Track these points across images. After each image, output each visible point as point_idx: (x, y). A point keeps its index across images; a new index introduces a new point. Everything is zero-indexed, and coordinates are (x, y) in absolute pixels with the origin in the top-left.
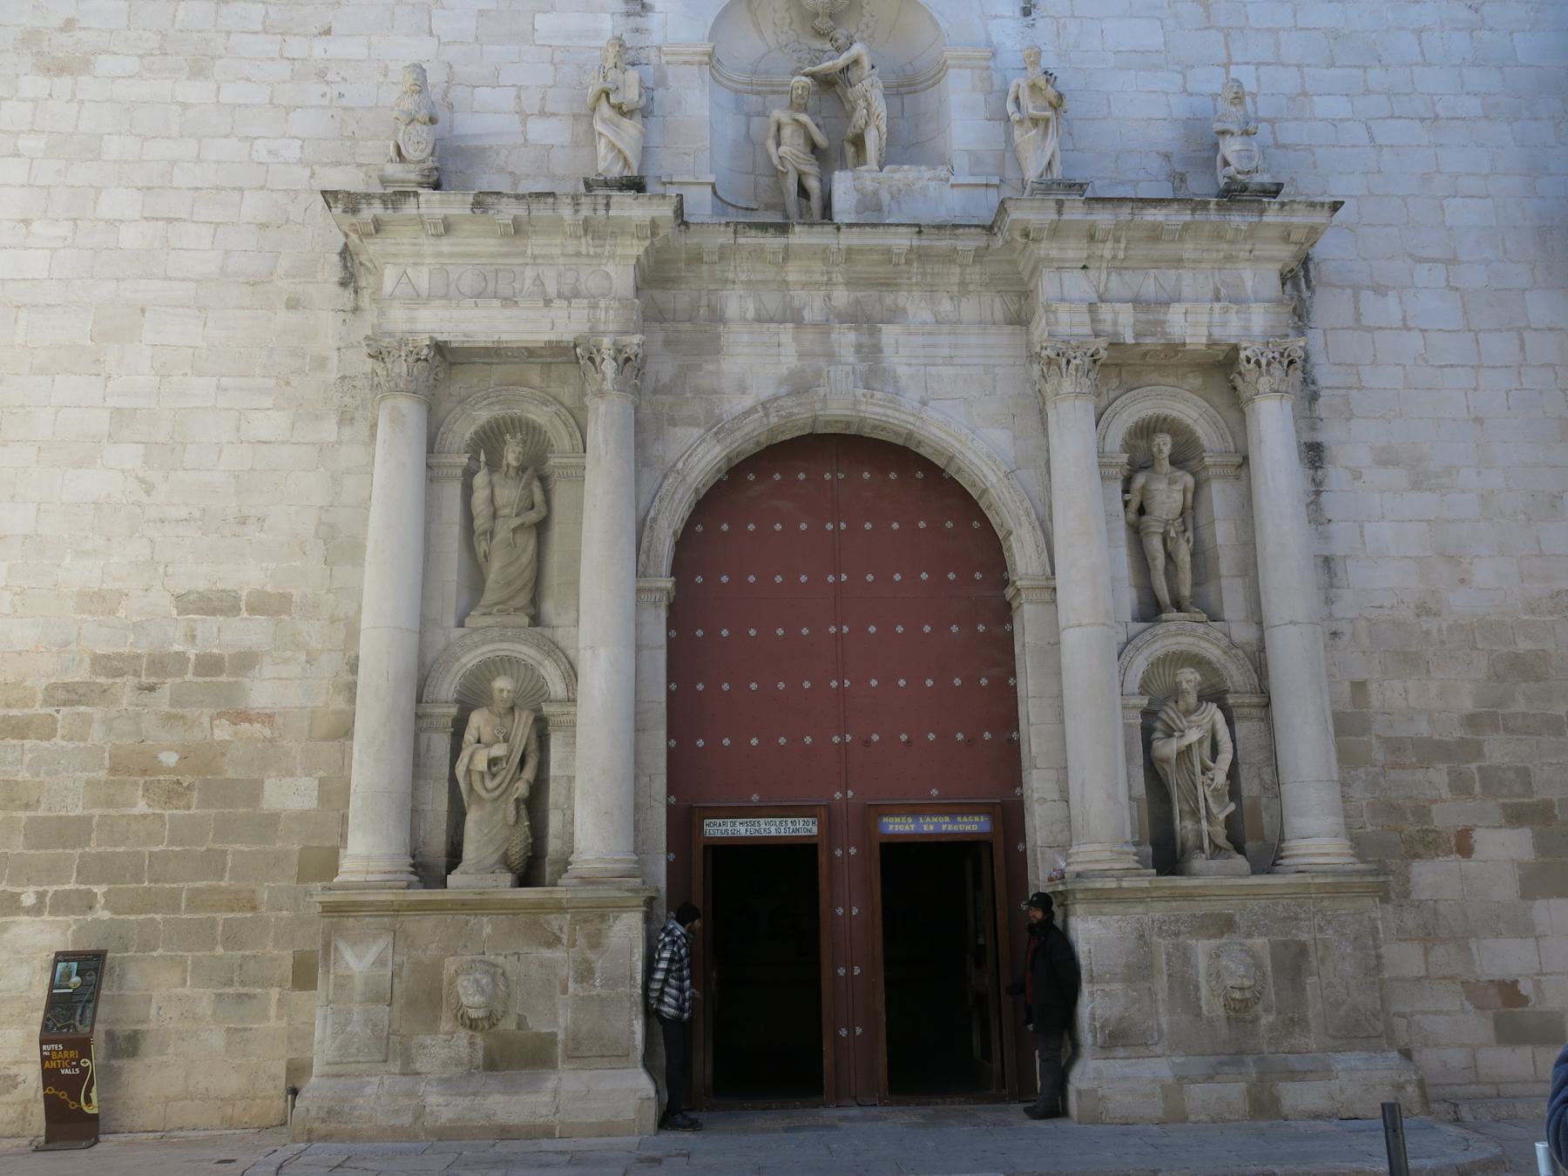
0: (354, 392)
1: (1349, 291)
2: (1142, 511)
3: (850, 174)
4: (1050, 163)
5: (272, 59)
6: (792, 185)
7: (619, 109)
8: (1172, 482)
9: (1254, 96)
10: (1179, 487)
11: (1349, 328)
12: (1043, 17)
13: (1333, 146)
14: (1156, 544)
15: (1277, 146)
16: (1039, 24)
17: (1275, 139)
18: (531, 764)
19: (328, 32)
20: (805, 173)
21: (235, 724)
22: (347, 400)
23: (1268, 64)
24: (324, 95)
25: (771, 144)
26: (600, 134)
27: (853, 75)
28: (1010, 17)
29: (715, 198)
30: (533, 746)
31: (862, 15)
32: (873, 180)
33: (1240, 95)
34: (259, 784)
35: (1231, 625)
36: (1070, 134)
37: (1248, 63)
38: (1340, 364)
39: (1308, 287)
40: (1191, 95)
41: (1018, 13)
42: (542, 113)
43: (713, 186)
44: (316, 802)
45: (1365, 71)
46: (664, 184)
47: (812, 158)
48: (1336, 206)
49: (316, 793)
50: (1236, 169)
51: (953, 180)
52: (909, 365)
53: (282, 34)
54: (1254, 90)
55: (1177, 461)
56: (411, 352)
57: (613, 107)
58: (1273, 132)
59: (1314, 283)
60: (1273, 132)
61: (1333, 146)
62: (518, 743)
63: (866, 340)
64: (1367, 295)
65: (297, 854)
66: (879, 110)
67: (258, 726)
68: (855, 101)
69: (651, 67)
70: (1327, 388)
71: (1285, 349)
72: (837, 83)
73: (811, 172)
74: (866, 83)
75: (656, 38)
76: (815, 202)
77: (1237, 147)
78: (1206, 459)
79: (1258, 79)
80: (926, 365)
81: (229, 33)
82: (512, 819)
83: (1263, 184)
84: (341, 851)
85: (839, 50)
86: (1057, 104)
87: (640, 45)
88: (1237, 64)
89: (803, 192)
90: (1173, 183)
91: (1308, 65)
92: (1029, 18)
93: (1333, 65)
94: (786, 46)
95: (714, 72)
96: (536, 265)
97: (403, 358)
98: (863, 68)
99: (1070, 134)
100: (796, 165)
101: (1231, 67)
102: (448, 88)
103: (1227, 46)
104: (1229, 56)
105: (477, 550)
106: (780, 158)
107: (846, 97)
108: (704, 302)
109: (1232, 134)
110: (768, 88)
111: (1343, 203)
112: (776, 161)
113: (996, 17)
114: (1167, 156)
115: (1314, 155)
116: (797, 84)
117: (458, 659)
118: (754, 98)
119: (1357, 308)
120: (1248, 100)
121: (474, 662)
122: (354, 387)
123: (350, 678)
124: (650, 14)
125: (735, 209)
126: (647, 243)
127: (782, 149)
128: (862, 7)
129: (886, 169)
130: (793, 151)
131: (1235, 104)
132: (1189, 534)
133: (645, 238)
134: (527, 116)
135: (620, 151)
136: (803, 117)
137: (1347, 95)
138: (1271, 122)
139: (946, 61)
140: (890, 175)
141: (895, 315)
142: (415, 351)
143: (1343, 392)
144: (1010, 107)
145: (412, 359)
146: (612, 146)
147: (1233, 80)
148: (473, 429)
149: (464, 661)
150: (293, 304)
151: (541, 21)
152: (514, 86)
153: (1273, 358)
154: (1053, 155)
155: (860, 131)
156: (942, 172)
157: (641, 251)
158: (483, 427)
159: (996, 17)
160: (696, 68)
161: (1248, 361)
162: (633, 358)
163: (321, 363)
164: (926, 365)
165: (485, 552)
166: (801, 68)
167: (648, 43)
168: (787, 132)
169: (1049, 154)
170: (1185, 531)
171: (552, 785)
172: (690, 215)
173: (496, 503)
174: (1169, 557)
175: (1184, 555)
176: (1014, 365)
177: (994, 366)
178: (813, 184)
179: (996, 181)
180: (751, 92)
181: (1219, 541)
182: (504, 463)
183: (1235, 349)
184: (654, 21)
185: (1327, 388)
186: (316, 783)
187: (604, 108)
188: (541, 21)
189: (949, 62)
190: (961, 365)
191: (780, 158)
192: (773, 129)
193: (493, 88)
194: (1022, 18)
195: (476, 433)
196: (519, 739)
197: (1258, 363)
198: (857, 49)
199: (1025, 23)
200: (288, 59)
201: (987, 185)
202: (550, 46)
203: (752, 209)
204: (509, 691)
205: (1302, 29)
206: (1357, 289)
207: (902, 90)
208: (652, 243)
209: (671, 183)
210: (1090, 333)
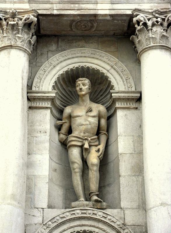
2: (70, 131)
8: (90, 110)
10: (95, 113)
14: (75, 153)
35: (126, 212)
55: (95, 99)
71: (166, 17)
78: (113, 95)
132: (102, 147)
153: (157, 22)
170: (99, 144)
174: (84, 161)
175: (94, 158)
181: (120, 151)
197: (145, 24)
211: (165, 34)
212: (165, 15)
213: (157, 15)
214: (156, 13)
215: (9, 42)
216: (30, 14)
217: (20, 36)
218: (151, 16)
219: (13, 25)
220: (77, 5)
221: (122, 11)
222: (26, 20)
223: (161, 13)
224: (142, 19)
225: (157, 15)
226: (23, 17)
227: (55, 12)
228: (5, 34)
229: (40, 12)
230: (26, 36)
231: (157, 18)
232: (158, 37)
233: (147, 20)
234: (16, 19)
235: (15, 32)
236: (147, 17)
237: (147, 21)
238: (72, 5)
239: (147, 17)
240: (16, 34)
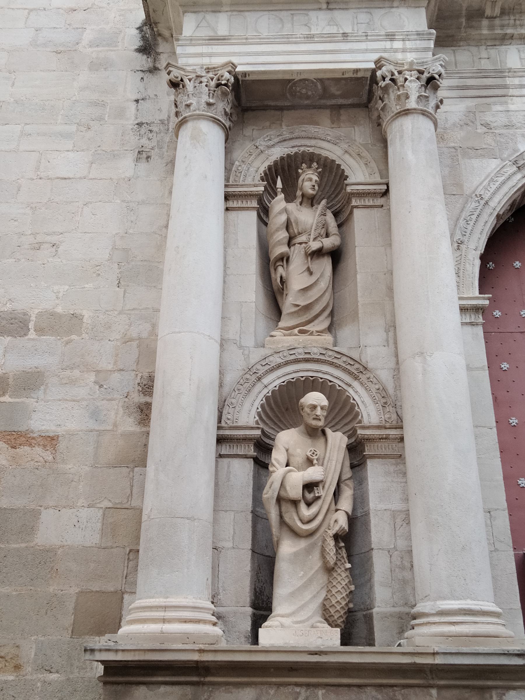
0: (150, 135)
18: (347, 494)
21: (14, 447)
22: (144, 141)
30: (348, 473)
34: (35, 514)
44: (99, 536)
49: (99, 525)
62: (333, 468)
65: (74, 599)
67: (38, 450)
82: (332, 562)
84: (126, 596)
96: (330, 9)
105: (273, 275)
117: (259, 379)
121: (278, 382)
122: (151, 131)
123: (144, 399)
145: (213, 83)
148: (266, 164)
149: (266, 380)
158: (276, 163)
162: (437, 77)
165: (281, 277)
171: (374, 521)
173: (291, 231)
182: (299, 193)
186: (100, 513)
195: (270, 168)
196: (334, 463)
204: (322, 408)
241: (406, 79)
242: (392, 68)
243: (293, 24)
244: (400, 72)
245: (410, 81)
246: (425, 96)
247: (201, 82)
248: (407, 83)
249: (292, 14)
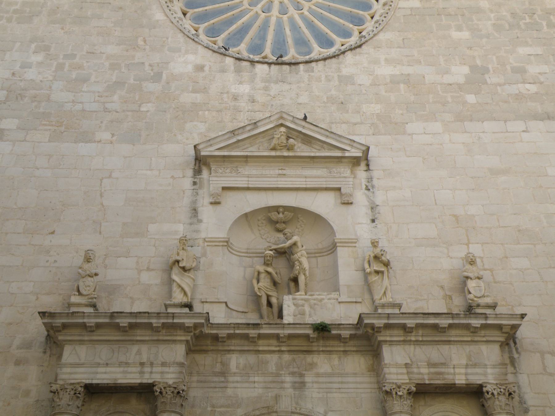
1: (538, 355)
3: (291, 296)
4: (385, 292)
5: (25, 245)
6: (264, 301)
7: (184, 269)
9: (481, 258)
11: (541, 373)
12: (380, 223)
13: (523, 282)
15: (495, 282)
16: (379, 226)
17: (494, 279)
19: (53, 233)
20: (271, 296)
23: (487, 243)
24: (47, 261)
25: (255, 282)
26: (174, 281)
27: (295, 249)
28: (366, 223)
29: (227, 308)
31: (299, 222)
32: (302, 299)
33: (473, 260)
36: (395, 277)
37: (478, 243)
38: (538, 393)
39: (518, 352)
40: (452, 258)
41: (369, 222)
42: (148, 269)
43: (226, 303)
45: (535, 246)
46: (203, 302)
47: (273, 288)
48: (523, 316)
50: (474, 295)
51: (340, 300)
52: (319, 393)
53: (32, 234)
54: (482, 256)
56: (72, 389)
57: (181, 267)
58: (493, 275)
59: (520, 350)
60: (493, 275)
61: (523, 282)
63: (297, 379)
64: (548, 356)
66: (305, 266)
68: (294, 262)
69: (200, 248)
70: (533, 406)
71: (506, 387)
72: (287, 252)
73: (273, 295)
74: (299, 254)
75: (203, 235)
76: (275, 309)
77: (474, 285)
79: (483, 250)
80: (327, 393)
81: (7, 234)
83: (487, 303)
85: (287, 239)
86: (387, 264)
87: (196, 238)
88: (472, 243)
89: (269, 304)
90: (446, 300)
91: (507, 244)
92: (374, 224)
93: (519, 243)
94: (264, 235)
95: (229, 249)
97: (68, 393)
98: (298, 247)
99: (395, 277)
100: (266, 292)
101: (470, 245)
102: (106, 258)
103: (467, 236)
104: (468, 240)
106: (259, 288)
107: (290, 259)
108: (219, 360)
109: (471, 279)
110: (255, 255)
111: (526, 315)
112: (256, 289)
113: (359, 223)
114: (442, 287)
115: (513, 286)
116: (267, 255)
118: (248, 259)
119: (543, 363)
120: (478, 260)
124: (201, 224)
125: (237, 312)
126: (192, 334)
127: (260, 284)
128: (298, 219)
129: (309, 293)
130: (266, 286)
131: (471, 265)
133: (191, 332)
134: (141, 271)
135: (183, 289)
136: (270, 269)
137: (527, 257)
138: (491, 270)
139: (336, 244)
140: (310, 297)
141: (312, 365)
142: (74, 389)
143: (542, 408)
144: (367, 266)
145: (72, 392)
146: (180, 286)
147: (470, 253)
150: (18, 363)
151: (152, 228)
152: (136, 256)
153: (501, 392)
154: (386, 289)
155: (296, 276)
156: (334, 295)
157: (189, 338)
159: (359, 223)
160: (220, 248)
161: (488, 393)
162: (181, 392)
163: (27, 393)
164: (327, 393)
166: (270, 247)
167: (199, 237)
168: (262, 276)
169: (385, 287)
172: (214, 317)
176: (371, 392)
177: (361, 393)
178: (274, 300)
179: (360, 300)
180: (247, 257)
183: (481, 386)
184: (203, 226)
185: (533, 406)
187: (176, 270)
188: (152, 228)
189: (338, 245)
190: (344, 393)
191: (259, 288)
192: (256, 274)
193: (127, 257)
194: (371, 224)
197: (493, 394)
198: (295, 238)
199: (372, 226)
200: (33, 245)
201: (356, 302)
202: (154, 238)
203: (245, 312)
205: (502, 227)
206: (542, 354)
207: (317, 255)
208: (194, 334)
209: (206, 302)
210: (408, 379)
211: (507, 403)
212: (506, 386)
213: (500, 387)
214: (500, 385)
215: (398, 408)
216: (411, 386)
217: (405, 402)
218: (495, 387)
219: (401, 396)
220: (441, 376)
221: (474, 381)
222: (408, 390)
223: (502, 385)
224: (490, 390)
225: (500, 387)
226: (406, 387)
227: (427, 382)
228: (395, 401)
229: (417, 382)
230: (409, 401)
231: (500, 389)
232: (503, 404)
233: (493, 390)
234: (401, 389)
235: (402, 400)
236: (492, 387)
237: (494, 392)
238: (438, 376)
239: (492, 387)
240: (403, 402)
241: (167, 393)
242: (161, 386)
243: (118, 353)
244: (165, 388)
245: (168, 395)
246: (175, 403)
247: (67, 392)
248: (166, 396)
249: (120, 347)
